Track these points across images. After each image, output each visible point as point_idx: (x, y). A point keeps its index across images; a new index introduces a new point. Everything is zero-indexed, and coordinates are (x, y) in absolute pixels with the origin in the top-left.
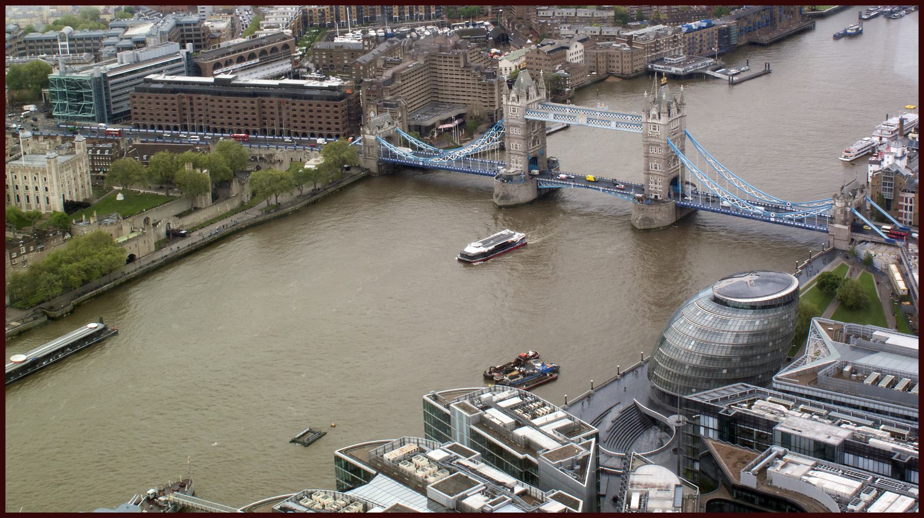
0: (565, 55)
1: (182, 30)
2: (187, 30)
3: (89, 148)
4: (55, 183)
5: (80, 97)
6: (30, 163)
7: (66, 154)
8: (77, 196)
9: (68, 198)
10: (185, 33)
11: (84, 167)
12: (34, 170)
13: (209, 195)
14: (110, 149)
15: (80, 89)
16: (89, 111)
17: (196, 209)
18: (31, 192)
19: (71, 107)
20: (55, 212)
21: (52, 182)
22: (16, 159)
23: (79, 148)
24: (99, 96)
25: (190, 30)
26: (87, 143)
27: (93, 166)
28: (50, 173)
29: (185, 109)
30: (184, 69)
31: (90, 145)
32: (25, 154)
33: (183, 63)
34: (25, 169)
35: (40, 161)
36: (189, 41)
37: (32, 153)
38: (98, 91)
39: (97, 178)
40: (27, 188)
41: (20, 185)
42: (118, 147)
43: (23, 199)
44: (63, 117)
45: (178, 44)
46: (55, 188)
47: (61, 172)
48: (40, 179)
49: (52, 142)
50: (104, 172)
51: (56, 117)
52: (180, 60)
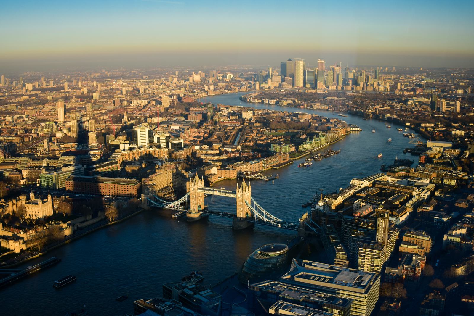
0: (210, 171)
1: (83, 161)
2: (85, 161)
4: (41, 210)
10: (84, 161)
13: (91, 217)
17: (87, 220)
21: (40, 210)
25: (85, 160)
28: (40, 207)
29: (83, 187)
30: (83, 173)
33: (83, 171)
36: (85, 164)
41: (30, 211)
45: (81, 165)
46: (41, 212)
47: (43, 207)
48: (36, 209)
52: (82, 170)
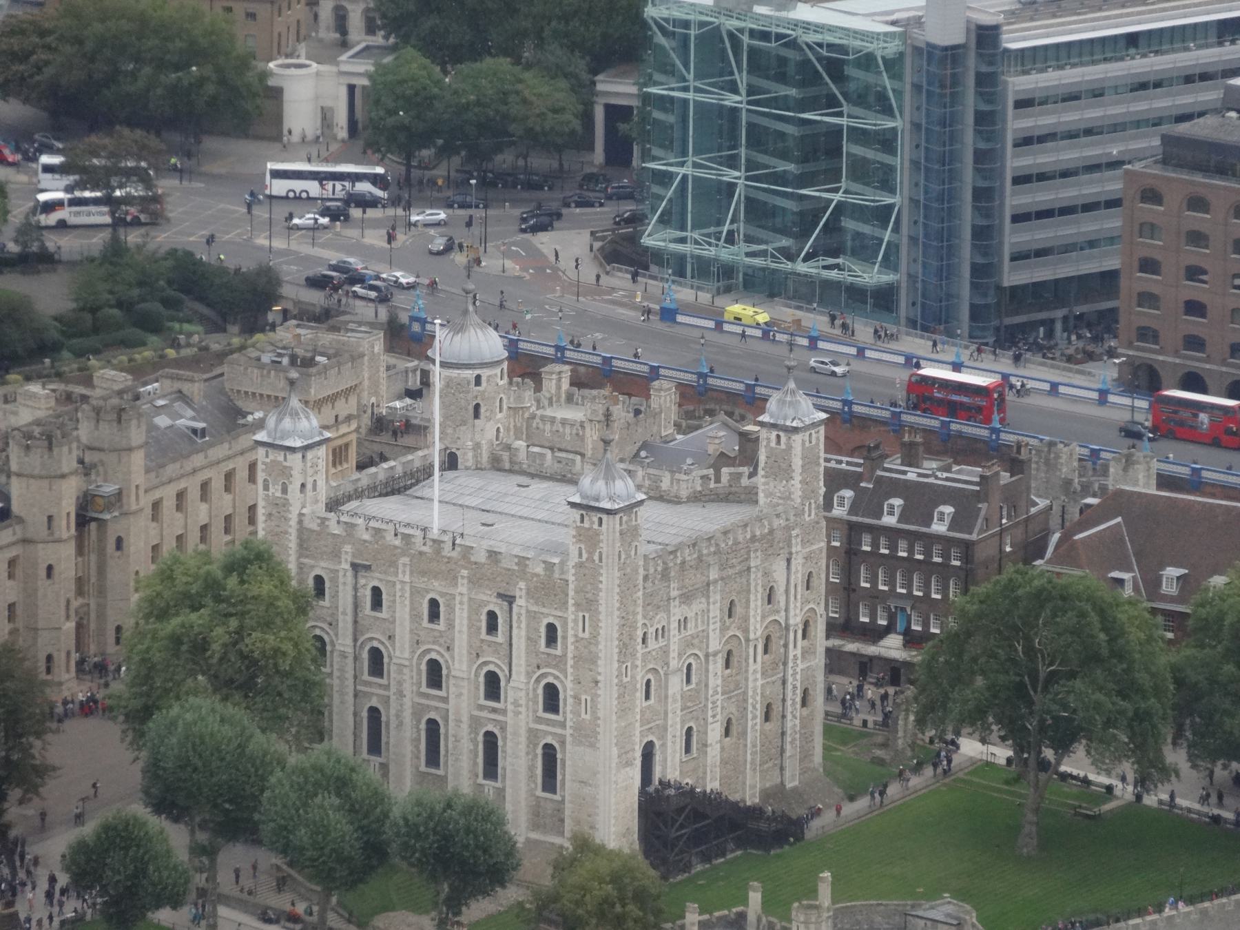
3: (835, 480)
5: (821, 152)
6: (471, 527)
7: (697, 498)
8: (732, 764)
9: (670, 767)
11: (796, 588)
12: (497, 574)
14: (966, 504)
15: (832, 102)
16: (864, 250)
18: (461, 699)
19: (757, 212)
20: (585, 845)
21: (587, 659)
22: (392, 488)
23: (781, 470)
24: (938, 163)
26: (833, 445)
27: (846, 592)
28: (589, 604)
31: (845, 463)
32: (451, 462)
34: (439, 558)
35: (525, 519)
37: (496, 465)
38: (938, 134)
39: (865, 666)
40: (435, 674)
42: (1014, 499)
43: (404, 741)
44: (704, 270)
47: (655, 604)
49: (621, 412)
50: (911, 640)
51: (658, 257)
